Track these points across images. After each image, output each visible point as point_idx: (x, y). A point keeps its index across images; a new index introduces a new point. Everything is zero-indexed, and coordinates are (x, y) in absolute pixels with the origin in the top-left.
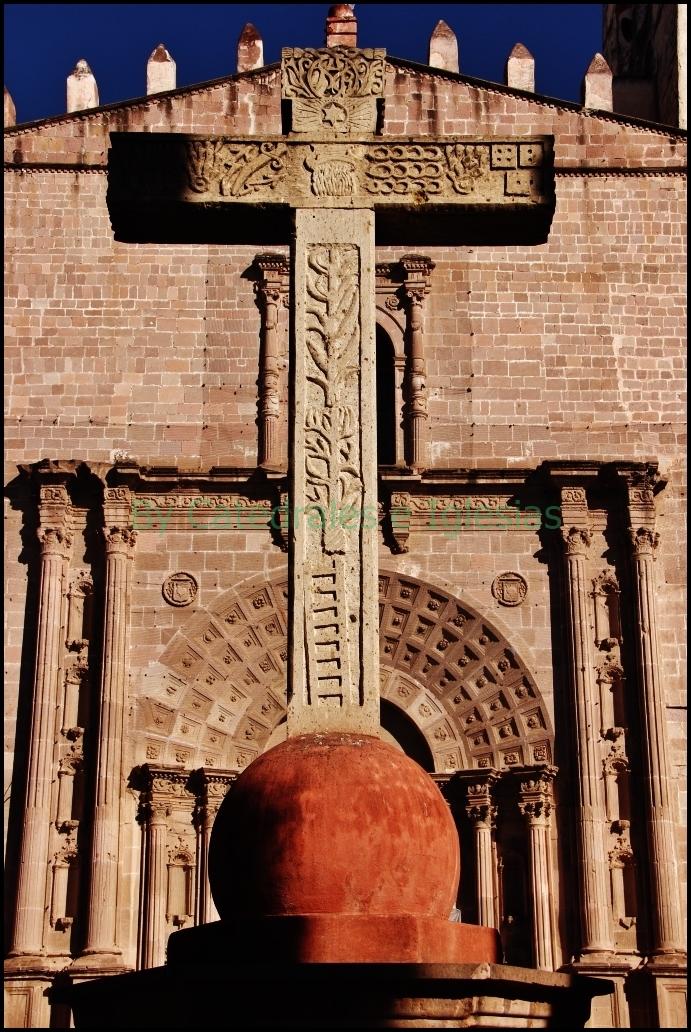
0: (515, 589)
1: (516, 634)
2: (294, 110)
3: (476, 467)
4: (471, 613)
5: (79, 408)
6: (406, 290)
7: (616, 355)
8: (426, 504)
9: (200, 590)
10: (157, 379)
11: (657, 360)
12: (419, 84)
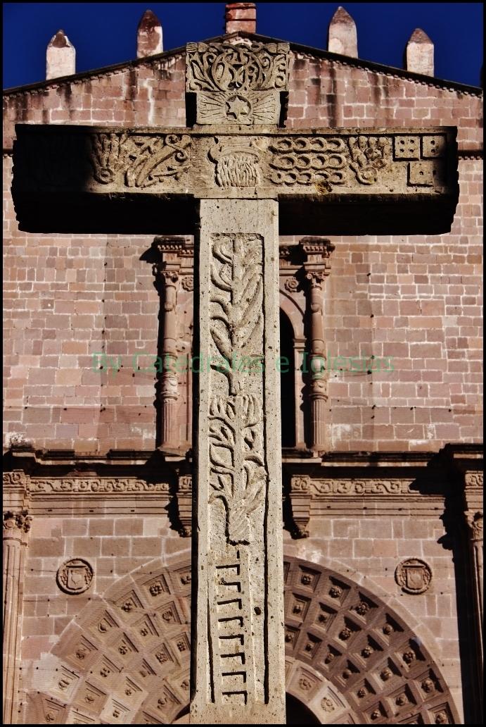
1: (420, 624)
2: (198, 103)
4: (374, 601)
6: (306, 272)
8: (326, 486)
9: (95, 577)
10: (54, 362)
12: (318, 70)
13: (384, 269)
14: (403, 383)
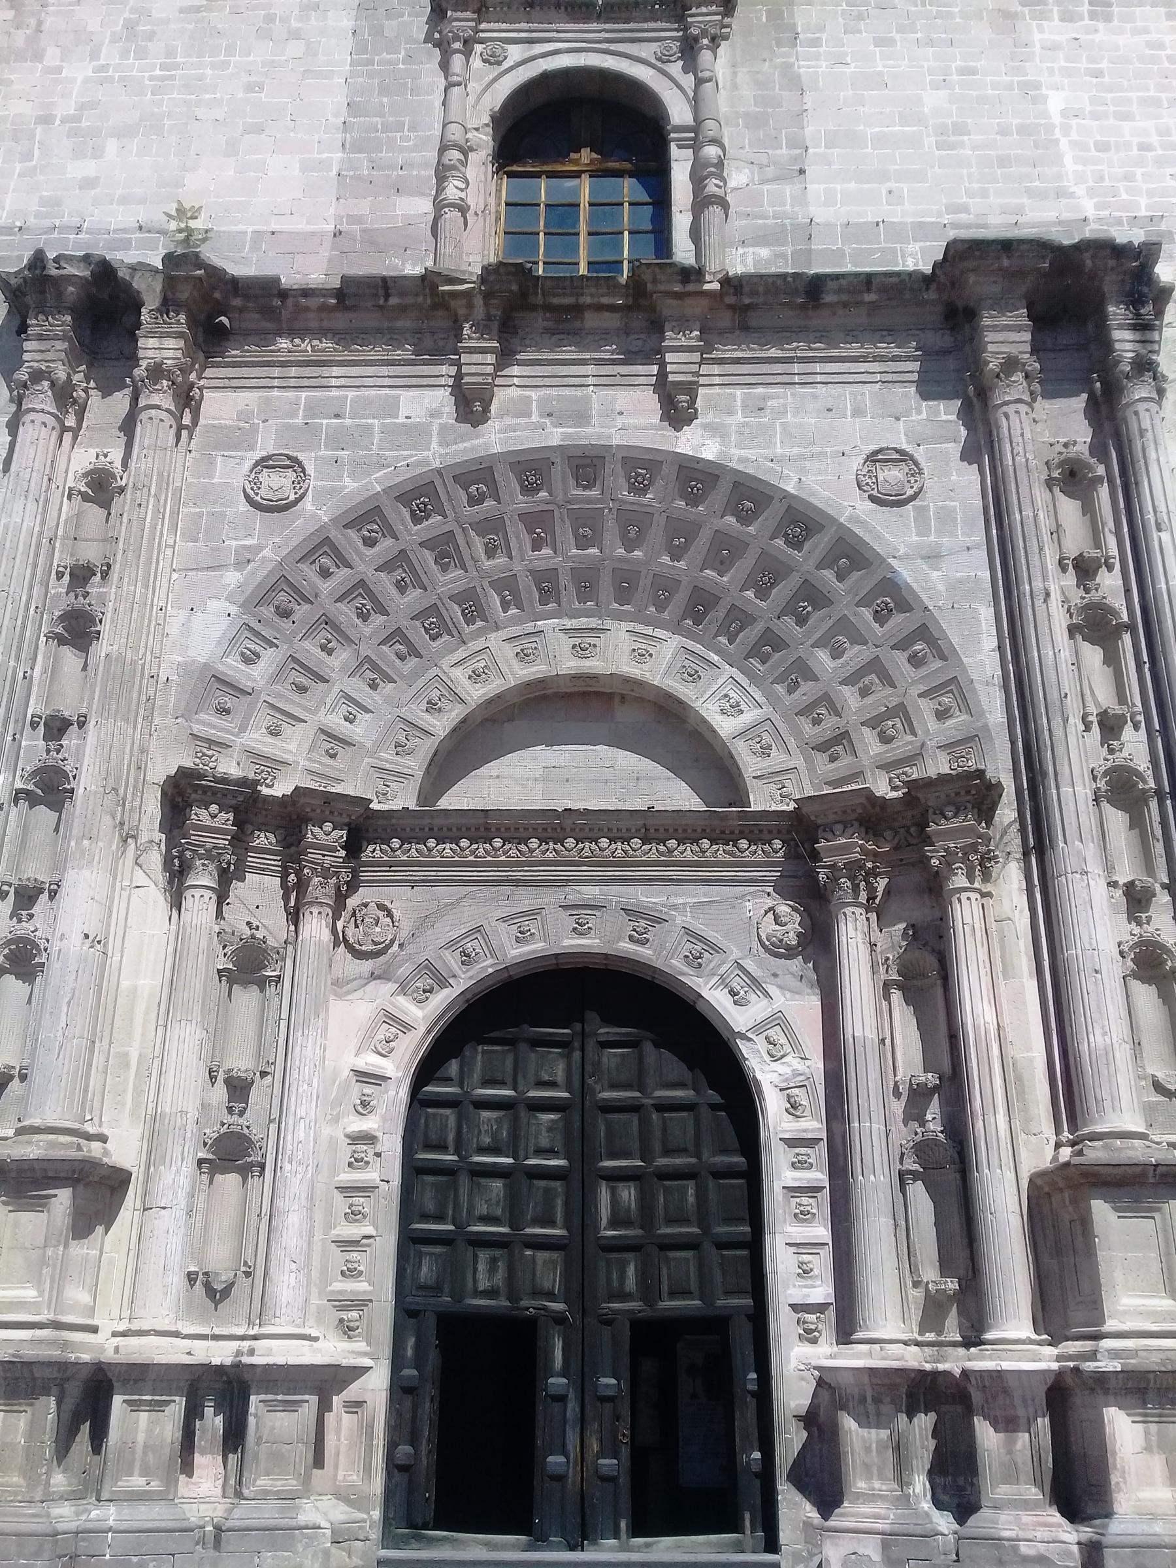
0: (900, 476)
5: (121, 208)
7: (1056, 119)
11: (1126, 126)
13: (822, 29)
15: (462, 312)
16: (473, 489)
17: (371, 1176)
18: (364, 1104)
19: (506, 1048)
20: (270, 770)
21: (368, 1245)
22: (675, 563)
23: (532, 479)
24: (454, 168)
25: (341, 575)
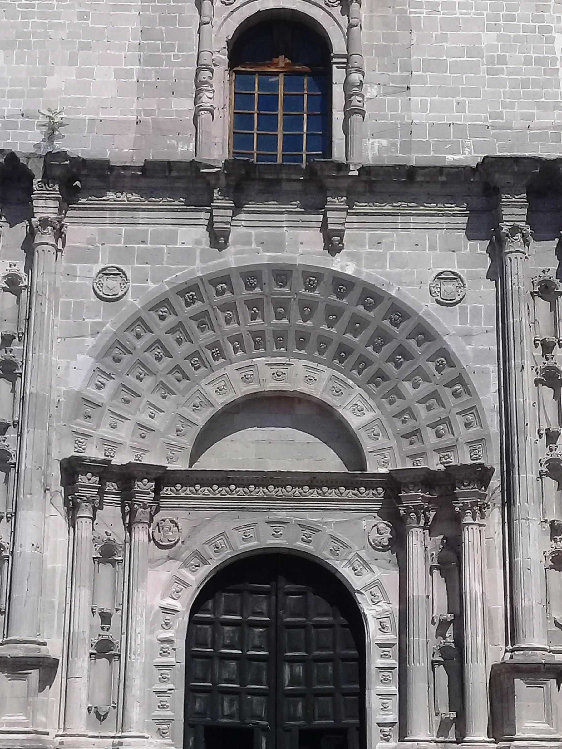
3: (414, 164)
14: (441, 98)
15: (213, 182)
16: (219, 287)
17: (171, 660)
18: (166, 624)
19: (237, 594)
20: (112, 447)
21: (171, 693)
22: (330, 329)
23: (252, 281)
24: (206, 82)
25: (147, 337)
